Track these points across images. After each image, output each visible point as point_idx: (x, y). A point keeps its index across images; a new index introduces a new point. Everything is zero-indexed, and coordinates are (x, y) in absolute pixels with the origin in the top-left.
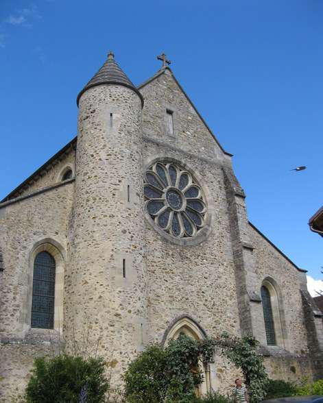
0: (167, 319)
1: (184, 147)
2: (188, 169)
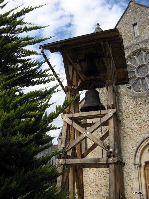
0: (138, 140)
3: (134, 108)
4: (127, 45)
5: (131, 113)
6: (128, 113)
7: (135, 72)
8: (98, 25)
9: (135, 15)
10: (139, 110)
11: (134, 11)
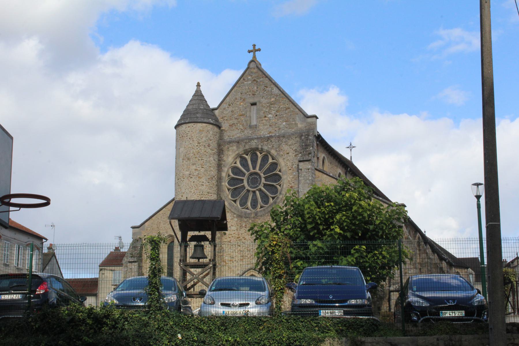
1: (264, 132)
3: (237, 230)
4: (238, 135)
5: (232, 237)
6: (230, 236)
8: (198, 85)
9: (255, 88)
10: (243, 235)
11: (254, 80)
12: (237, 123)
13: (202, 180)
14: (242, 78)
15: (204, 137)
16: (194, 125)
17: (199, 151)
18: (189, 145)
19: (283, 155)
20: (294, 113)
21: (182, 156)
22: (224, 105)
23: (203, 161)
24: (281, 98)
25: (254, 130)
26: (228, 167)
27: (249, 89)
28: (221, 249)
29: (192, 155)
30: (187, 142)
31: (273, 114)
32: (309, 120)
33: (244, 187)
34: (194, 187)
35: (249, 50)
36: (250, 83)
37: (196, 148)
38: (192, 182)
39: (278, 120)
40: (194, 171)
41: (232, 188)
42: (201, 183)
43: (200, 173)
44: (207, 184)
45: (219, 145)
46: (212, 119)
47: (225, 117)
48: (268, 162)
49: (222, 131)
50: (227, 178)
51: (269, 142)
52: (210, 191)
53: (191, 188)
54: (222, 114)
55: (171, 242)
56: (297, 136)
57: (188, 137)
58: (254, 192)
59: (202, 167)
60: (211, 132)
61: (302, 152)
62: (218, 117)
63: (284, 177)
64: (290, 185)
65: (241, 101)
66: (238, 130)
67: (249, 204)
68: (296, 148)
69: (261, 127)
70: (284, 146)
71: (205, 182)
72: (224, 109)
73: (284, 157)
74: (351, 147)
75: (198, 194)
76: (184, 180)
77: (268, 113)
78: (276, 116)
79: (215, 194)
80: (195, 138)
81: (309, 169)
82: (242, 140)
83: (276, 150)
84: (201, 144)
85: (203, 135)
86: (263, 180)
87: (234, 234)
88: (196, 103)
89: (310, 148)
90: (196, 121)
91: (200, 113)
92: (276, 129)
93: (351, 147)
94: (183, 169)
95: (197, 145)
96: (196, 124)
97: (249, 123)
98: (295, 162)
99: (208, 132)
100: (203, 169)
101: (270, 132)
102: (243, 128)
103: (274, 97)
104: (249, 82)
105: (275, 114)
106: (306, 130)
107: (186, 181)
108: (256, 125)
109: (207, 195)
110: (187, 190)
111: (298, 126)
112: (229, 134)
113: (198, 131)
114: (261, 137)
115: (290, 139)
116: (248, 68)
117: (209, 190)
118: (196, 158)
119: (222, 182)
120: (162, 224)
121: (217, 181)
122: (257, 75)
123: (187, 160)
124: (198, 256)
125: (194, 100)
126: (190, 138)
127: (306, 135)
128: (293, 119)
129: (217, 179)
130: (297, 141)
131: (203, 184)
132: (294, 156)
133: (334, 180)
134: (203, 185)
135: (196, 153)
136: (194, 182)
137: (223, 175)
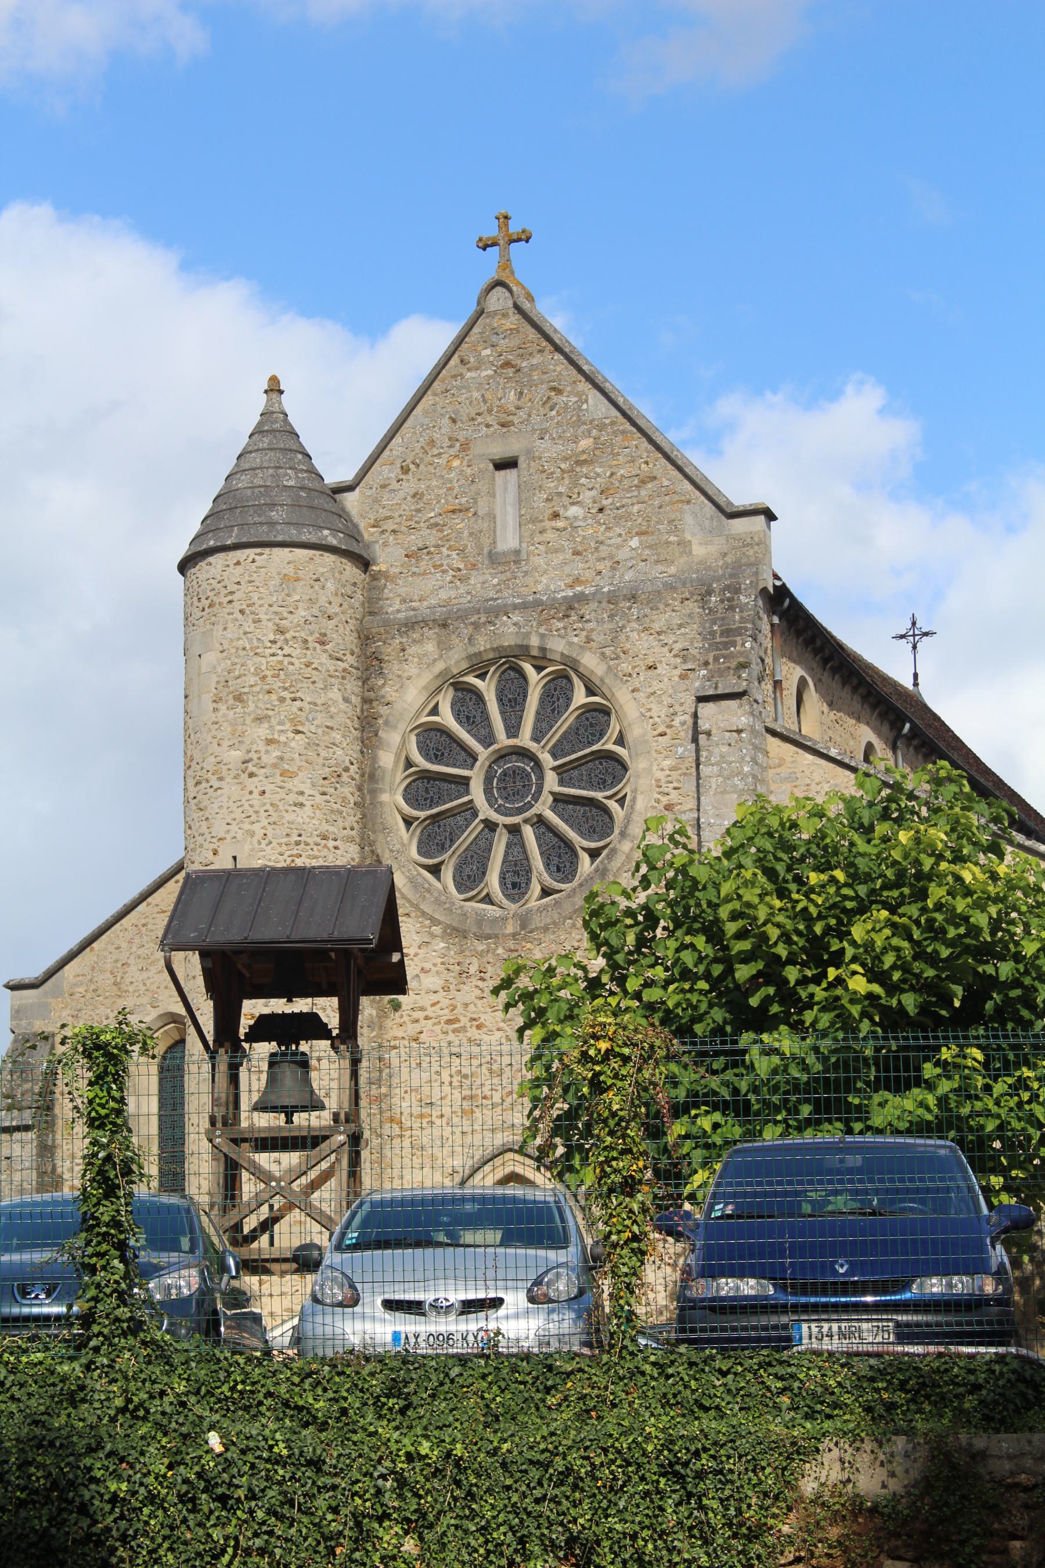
2: (558, 658)
3: (446, 989)
4: (443, 595)
5: (427, 1018)
7: (473, 784)
8: (274, 388)
10: (472, 1008)
11: (507, 364)
12: (437, 546)
13: (296, 784)
14: (456, 356)
15: (300, 604)
16: (261, 554)
17: (281, 662)
18: (239, 639)
19: (630, 675)
20: (676, 498)
21: (214, 685)
22: (382, 471)
23: (298, 703)
24: (620, 438)
25: (508, 574)
26: (403, 726)
27: (485, 401)
28: (380, 1071)
29: (252, 680)
30: (230, 625)
31: (589, 502)
32: (739, 525)
33: (471, 809)
34: (263, 814)
35: (480, 240)
36: (489, 377)
37: (268, 651)
38: (256, 795)
39: (608, 529)
40: (262, 747)
41: (423, 814)
42: (292, 798)
43: (287, 756)
44: (319, 799)
45: (365, 638)
46: (334, 530)
47: (387, 518)
48: (568, 706)
49: (374, 578)
50: (400, 775)
51: (575, 622)
52: (331, 829)
53: (254, 818)
54: (376, 507)
55: (172, 1041)
56: (687, 595)
57: (237, 606)
58: (514, 830)
59: (299, 732)
60: (329, 585)
61: (711, 660)
62: (356, 519)
63: (637, 765)
64: (665, 800)
65: (452, 451)
66: (444, 572)
67: (493, 880)
68: (687, 644)
69: (539, 561)
70: (634, 635)
71: (308, 792)
72: (384, 486)
73: (635, 682)
74: (914, 635)
75: (280, 844)
76: (223, 784)
77: (565, 499)
78: (601, 510)
79: (352, 840)
80: (264, 609)
81: (739, 731)
82: (462, 616)
83: (603, 654)
84: (288, 636)
85: (297, 597)
86: (551, 781)
87: (433, 1005)
88: (265, 464)
89: (743, 644)
90: (265, 538)
91: (282, 505)
92: (600, 566)
93: (914, 635)
94: (215, 741)
95: (272, 638)
96: (267, 550)
97: (486, 542)
98: (682, 704)
99: (317, 585)
100: (298, 737)
101: (577, 581)
102: (462, 566)
103: (589, 432)
104: (485, 373)
105: (597, 506)
106: (726, 566)
107: (230, 789)
108: (517, 552)
109: (318, 844)
110: (234, 827)
111: (690, 552)
112: (402, 591)
113: (276, 581)
114: (538, 603)
115: (661, 606)
116: (480, 313)
117: (326, 827)
118: (269, 692)
119: (382, 791)
120: (133, 969)
121: (360, 789)
122: (515, 342)
123: (231, 701)
124: (288, 1102)
125: (258, 450)
126: (242, 612)
127: (727, 588)
128: (670, 522)
129: (357, 777)
130: (690, 615)
131: (301, 799)
132: (677, 679)
133: (848, 773)
134: (302, 805)
135: (269, 673)
136: (264, 792)
137: (381, 764)
